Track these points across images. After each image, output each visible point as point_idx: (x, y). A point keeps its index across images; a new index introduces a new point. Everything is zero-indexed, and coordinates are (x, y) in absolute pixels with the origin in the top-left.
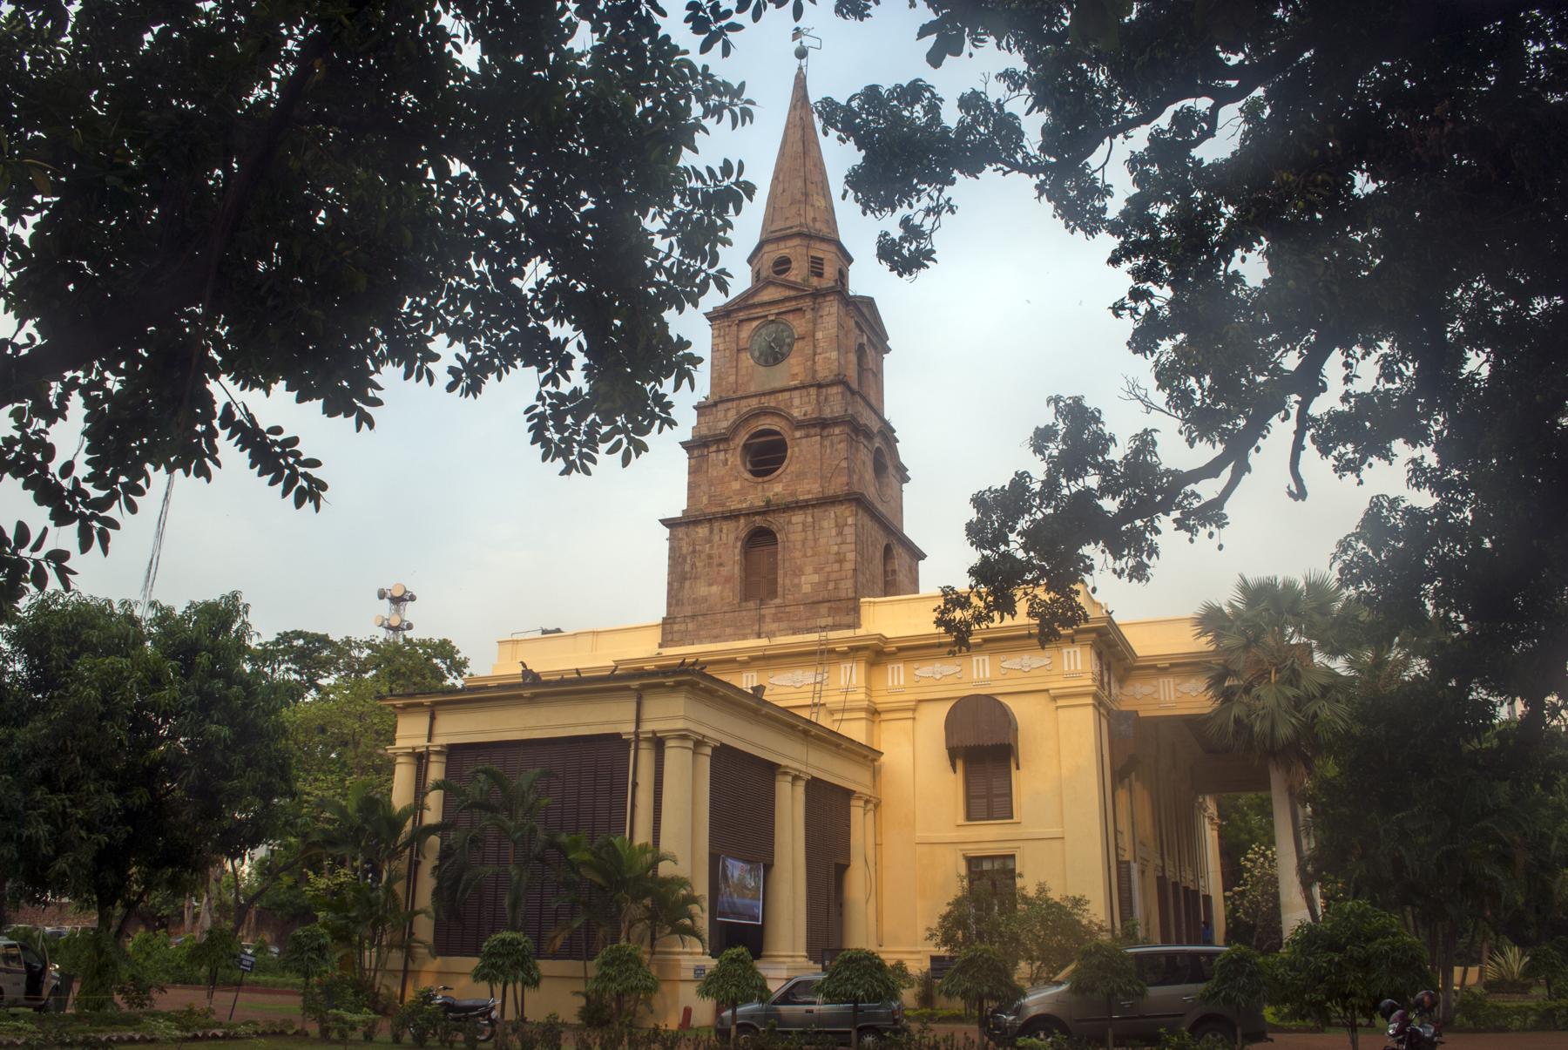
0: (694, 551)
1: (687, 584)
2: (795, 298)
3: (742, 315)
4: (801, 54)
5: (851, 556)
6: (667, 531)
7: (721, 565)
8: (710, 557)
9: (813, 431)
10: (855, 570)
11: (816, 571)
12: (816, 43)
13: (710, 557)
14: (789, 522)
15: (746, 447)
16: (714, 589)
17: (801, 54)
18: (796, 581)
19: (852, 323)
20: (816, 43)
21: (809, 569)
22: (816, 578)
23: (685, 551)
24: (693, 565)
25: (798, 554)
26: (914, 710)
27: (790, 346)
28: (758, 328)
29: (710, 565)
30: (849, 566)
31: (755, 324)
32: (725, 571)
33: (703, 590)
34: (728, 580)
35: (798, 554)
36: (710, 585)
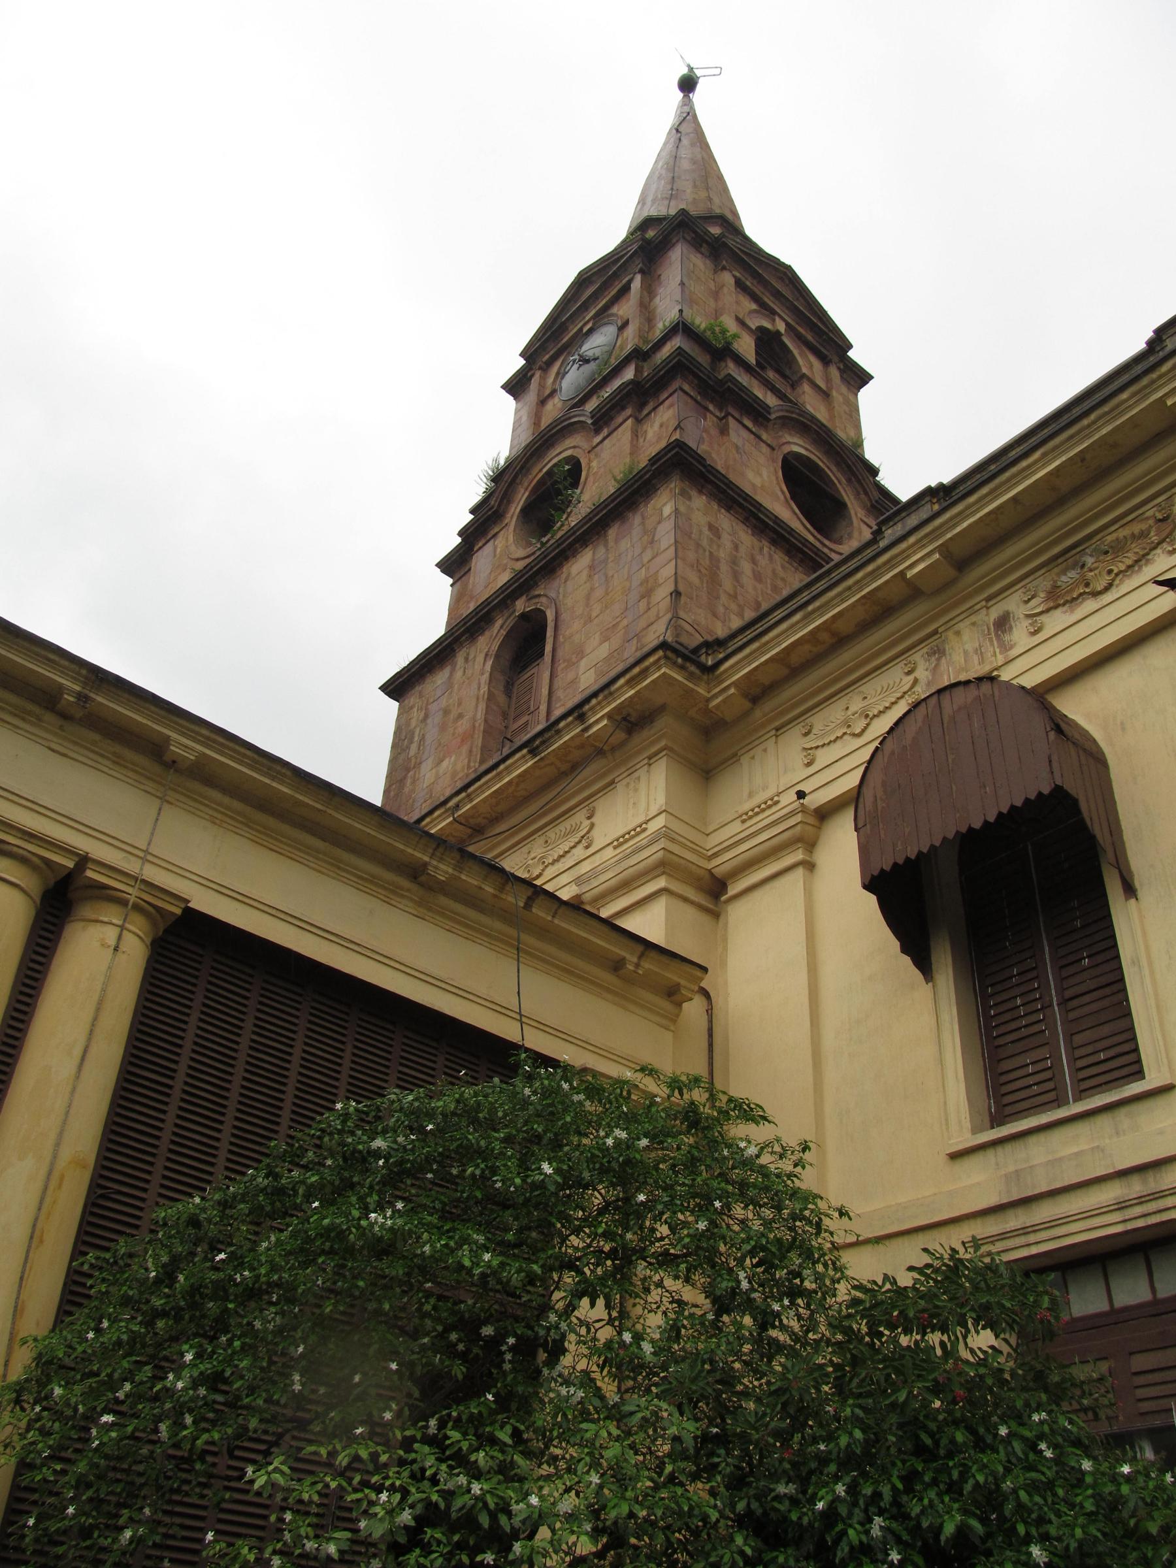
0: (426, 716)
4: (688, 84)
5: (669, 571)
6: (395, 705)
7: (460, 716)
10: (676, 594)
11: (606, 639)
12: (717, 71)
13: (446, 712)
15: (526, 511)
16: (445, 764)
17: (688, 84)
19: (728, 278)
20: (717, 71)
23: (413, 723)
25: (576, 625)
26: (810, 845)
30: (662, 594)
32: (463, 725)
34: (467, 737)
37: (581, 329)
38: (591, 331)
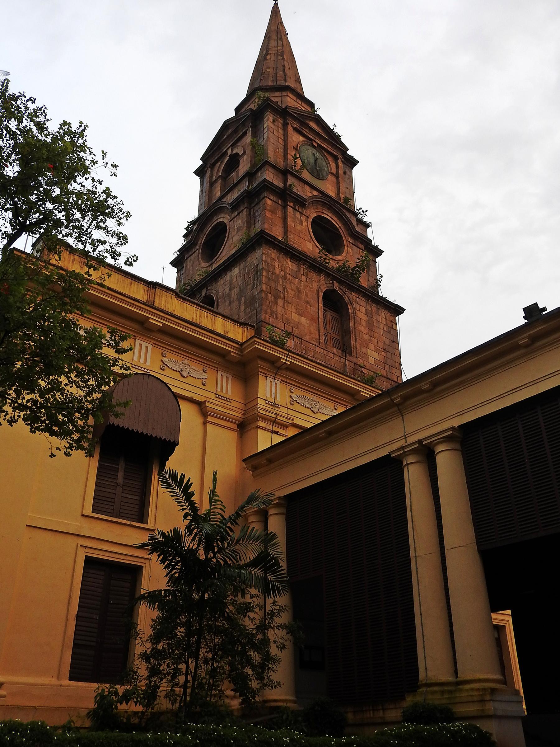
1: (280, 302)
2: (333, 145)
3: (296, 125)
8: (298, 290)
9: (361, 246)
11: (376, 351)
14: (356, 302)
16: (303, 320)
18: (364, 350)
21: (372, 346)
22: (376, 355)
23: (277, 271)
24: (285, 288)
27: (327, 175)
28: (304, 143)
29: (299, 297)
31: (302, 139)
33: (295, 317)
35: (362, 329)
36: (301, 315)
37: (311, 140)
38: (314, 147)
